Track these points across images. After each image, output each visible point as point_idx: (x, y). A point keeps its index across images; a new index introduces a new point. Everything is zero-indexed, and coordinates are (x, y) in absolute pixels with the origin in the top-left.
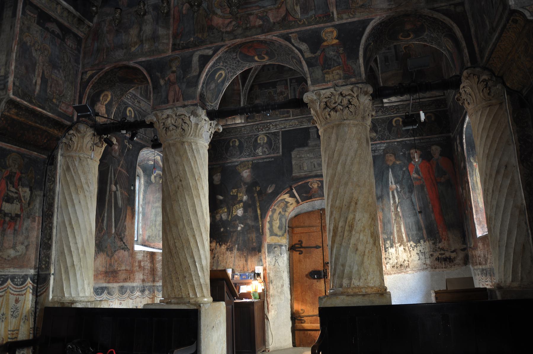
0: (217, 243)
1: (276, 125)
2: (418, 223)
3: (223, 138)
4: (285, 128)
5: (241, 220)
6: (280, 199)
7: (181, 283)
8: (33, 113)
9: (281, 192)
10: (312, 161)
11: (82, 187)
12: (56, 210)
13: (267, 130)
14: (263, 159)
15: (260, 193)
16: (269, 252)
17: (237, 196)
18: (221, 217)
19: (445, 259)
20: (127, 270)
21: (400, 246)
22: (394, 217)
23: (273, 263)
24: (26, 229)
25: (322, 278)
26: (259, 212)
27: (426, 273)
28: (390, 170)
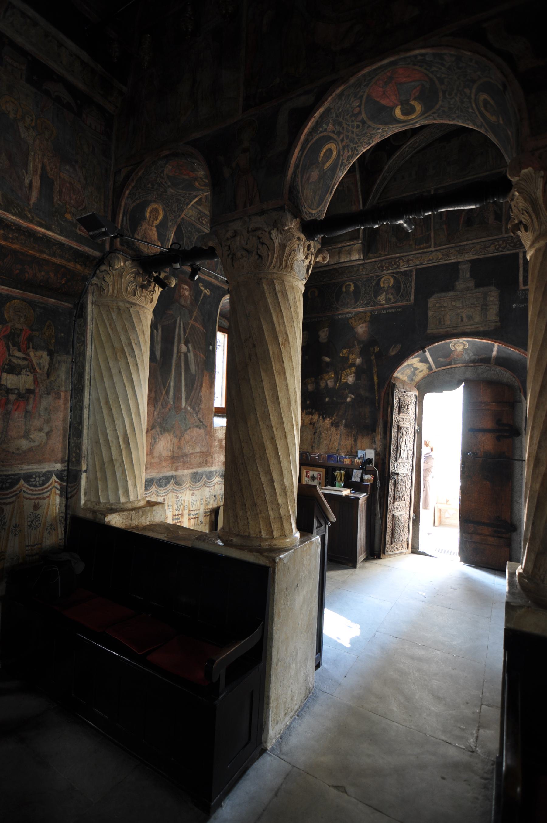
0: (320, 415)
1: (408, 261)
3: (334, 281)
4: (421, 264)
5: (352, 389)
6: (405, 364)
7: (249, 513)
8: (32, 234)
11: (123, 350)
12: (87, 382)
13: (395, 268)
14: (387, 309)
17: (348, 358)
18: (327, 384)
20: (203, 452)
24: (46, 409)
26: (376, 380)
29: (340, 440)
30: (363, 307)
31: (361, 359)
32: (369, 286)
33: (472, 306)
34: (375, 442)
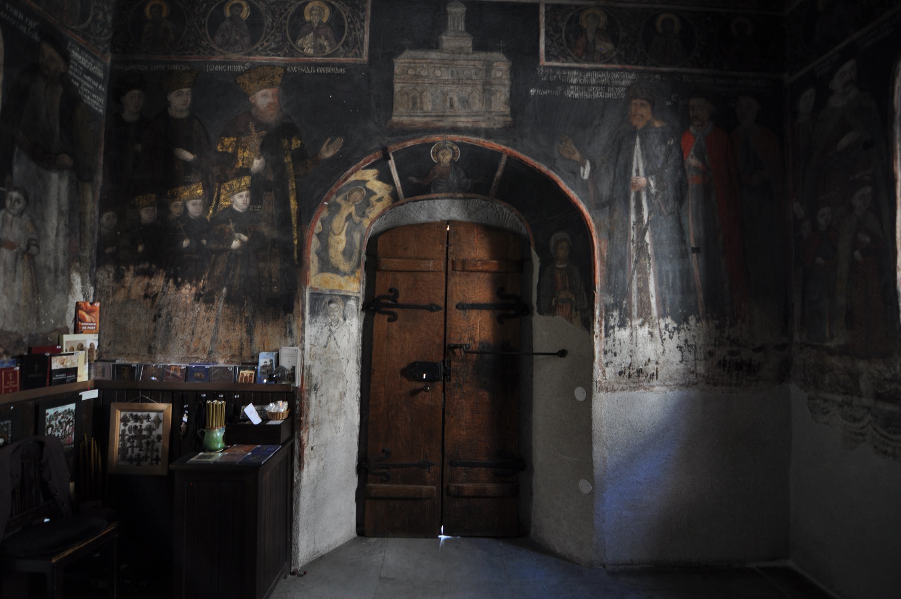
2: (685, 275)
5: (243, 221)
6: (352, 178)
9: (359, 159)
10: (446, 89)
14: (317, 65)
15: (300, 156)
16: (314, 313)
18: (186, 210)
19: (739, 366)
21: (642, 325)
22: (633, 253)
23: (322, 341)
25: (438, 380)
26: (293, 205)
27: (694, 393)
28: (638, 140)
29: (217, 331)
30: (268, 55)
31: (262, 159)
32: (281, 15)
33: (469, 82)
34: (291, 332)
